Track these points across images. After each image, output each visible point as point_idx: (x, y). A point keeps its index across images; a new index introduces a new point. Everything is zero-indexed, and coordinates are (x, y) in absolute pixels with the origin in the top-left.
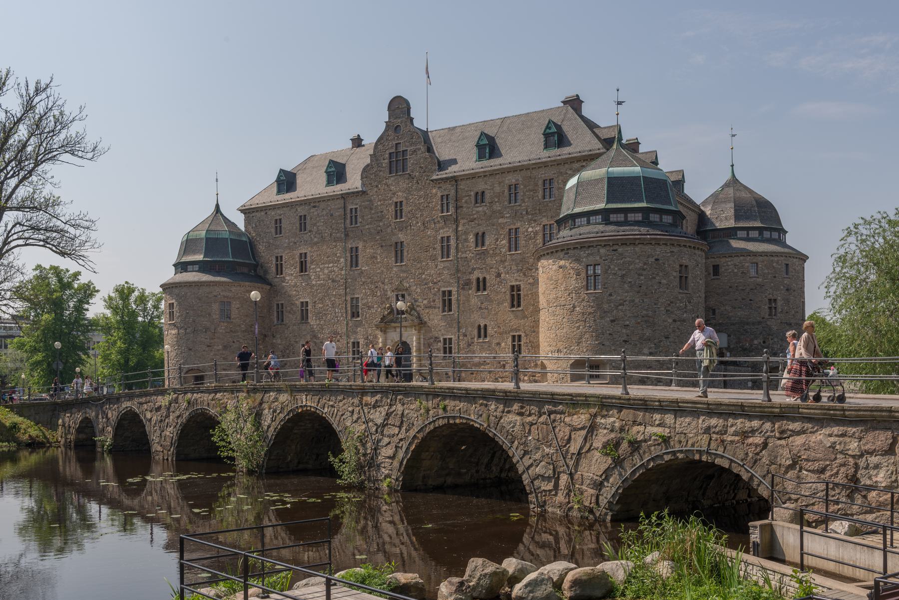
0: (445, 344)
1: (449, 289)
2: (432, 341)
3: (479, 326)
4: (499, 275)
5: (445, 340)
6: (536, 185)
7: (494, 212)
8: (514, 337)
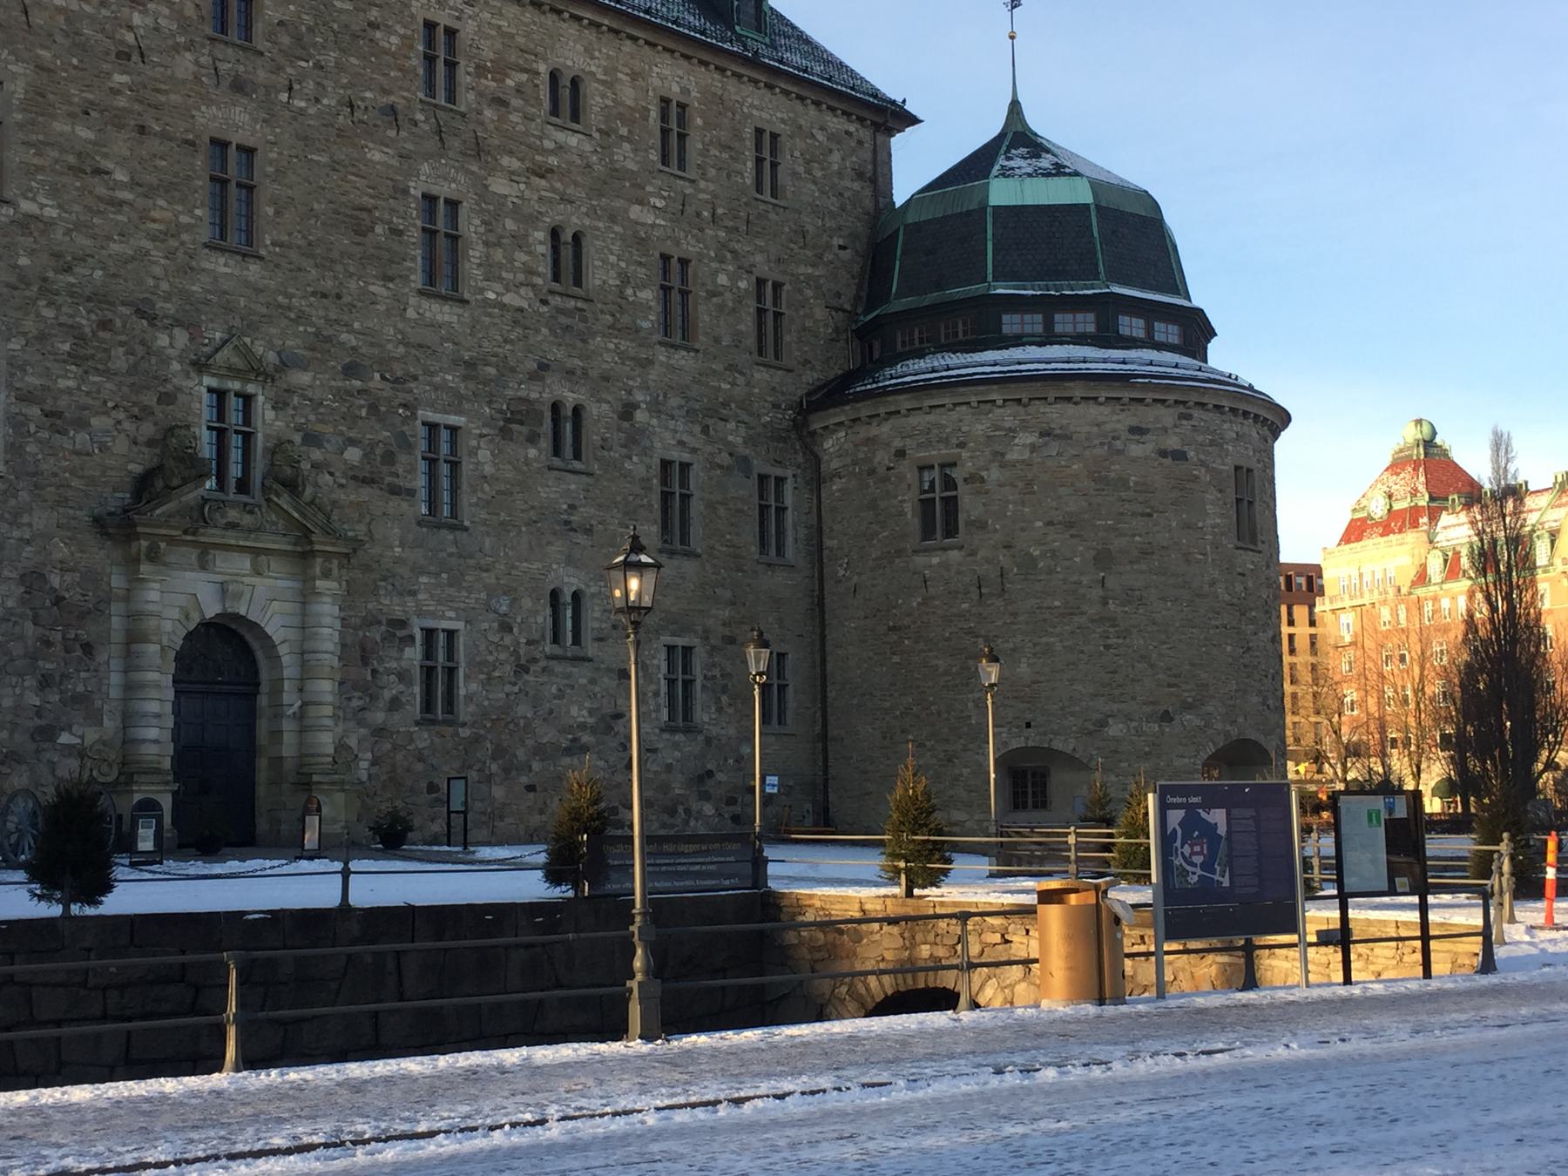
0: (429, 653)
1: (454, 420)
2: (376, 634)
3: (555, 595)
4: (627, 411)
5: (429, 634)
6: (737, 135)
7: (616, 173)
8: (671, 649)
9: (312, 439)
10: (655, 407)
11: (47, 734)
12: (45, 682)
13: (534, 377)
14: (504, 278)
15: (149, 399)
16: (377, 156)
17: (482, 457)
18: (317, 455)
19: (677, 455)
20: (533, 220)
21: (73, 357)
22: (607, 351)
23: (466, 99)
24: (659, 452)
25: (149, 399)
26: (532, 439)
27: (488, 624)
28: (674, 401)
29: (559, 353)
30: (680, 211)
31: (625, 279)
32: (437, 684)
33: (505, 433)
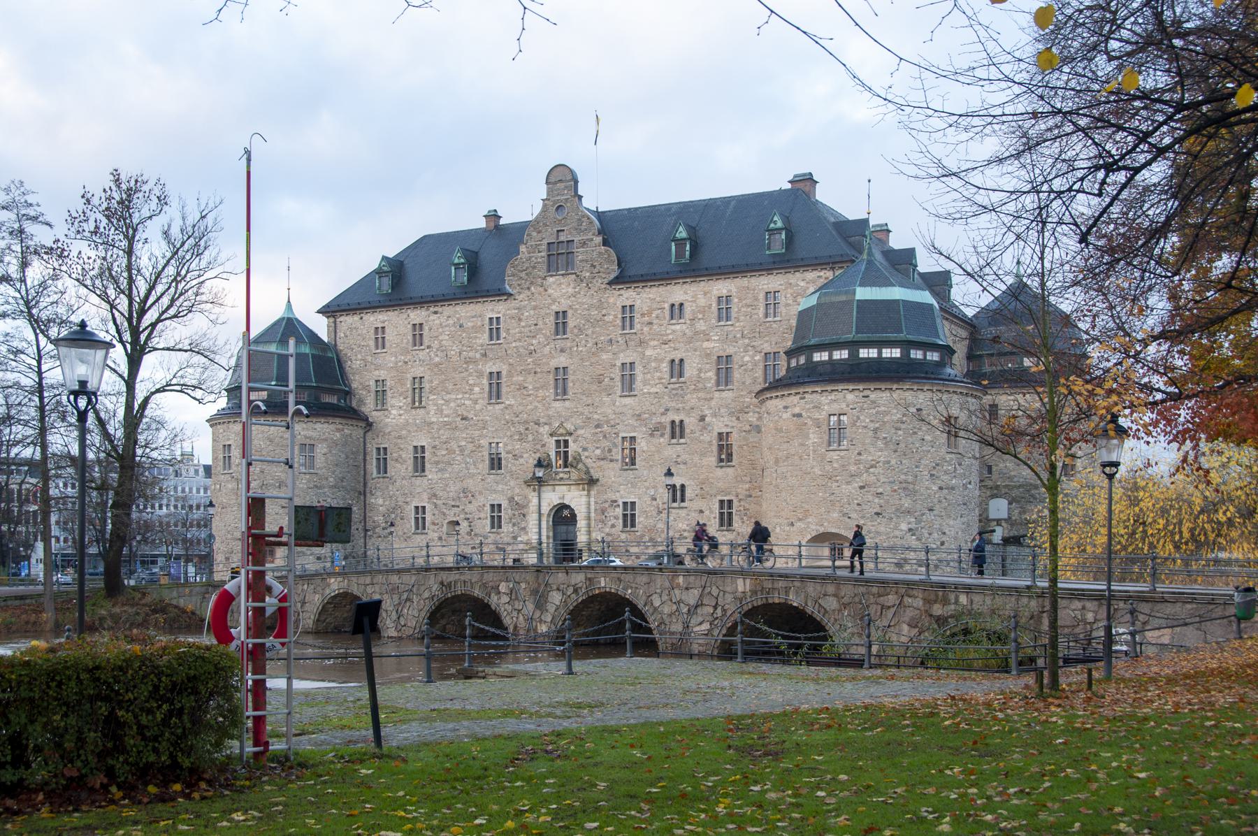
0: (625, 509)
1: (632, 434)
4: (702, 419)
7: (696, 333)
9: (585, 449)
10: (714, 415)
11: (515, 538)
12: (514, 525)
13: (662, 414)
14: (651, 382)
15: (538, 447)
16: (604, 357)
17: (641, 445)
18: (586, 454)
19: (724, 430)
20: (662, 361)
21: (520, 440)
22: (692, 399)
23: (637, 326)
24: (717, 430)
25: (538, 447)
26: (662, 435)
27: (647, 499)
28: (722, 410)
29: (673, 404)
30: (726, 339)
31: (700, 370)
32: (629, 520)
33: (652, 435)
